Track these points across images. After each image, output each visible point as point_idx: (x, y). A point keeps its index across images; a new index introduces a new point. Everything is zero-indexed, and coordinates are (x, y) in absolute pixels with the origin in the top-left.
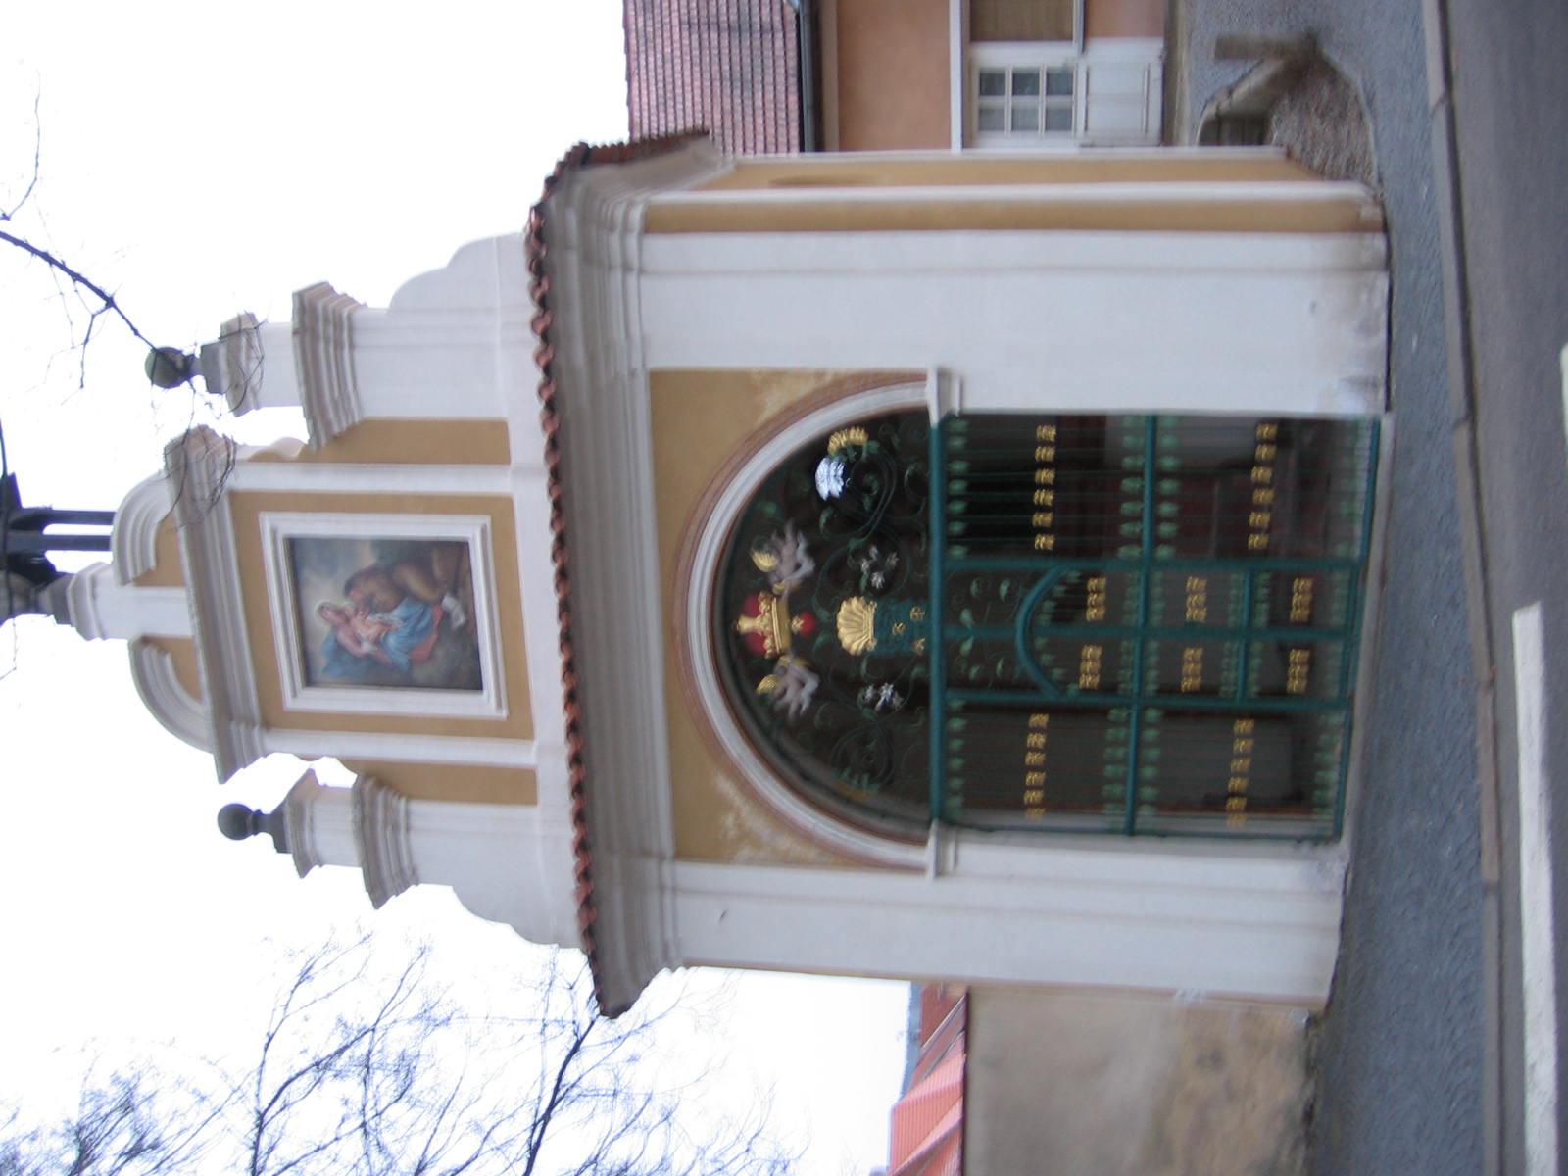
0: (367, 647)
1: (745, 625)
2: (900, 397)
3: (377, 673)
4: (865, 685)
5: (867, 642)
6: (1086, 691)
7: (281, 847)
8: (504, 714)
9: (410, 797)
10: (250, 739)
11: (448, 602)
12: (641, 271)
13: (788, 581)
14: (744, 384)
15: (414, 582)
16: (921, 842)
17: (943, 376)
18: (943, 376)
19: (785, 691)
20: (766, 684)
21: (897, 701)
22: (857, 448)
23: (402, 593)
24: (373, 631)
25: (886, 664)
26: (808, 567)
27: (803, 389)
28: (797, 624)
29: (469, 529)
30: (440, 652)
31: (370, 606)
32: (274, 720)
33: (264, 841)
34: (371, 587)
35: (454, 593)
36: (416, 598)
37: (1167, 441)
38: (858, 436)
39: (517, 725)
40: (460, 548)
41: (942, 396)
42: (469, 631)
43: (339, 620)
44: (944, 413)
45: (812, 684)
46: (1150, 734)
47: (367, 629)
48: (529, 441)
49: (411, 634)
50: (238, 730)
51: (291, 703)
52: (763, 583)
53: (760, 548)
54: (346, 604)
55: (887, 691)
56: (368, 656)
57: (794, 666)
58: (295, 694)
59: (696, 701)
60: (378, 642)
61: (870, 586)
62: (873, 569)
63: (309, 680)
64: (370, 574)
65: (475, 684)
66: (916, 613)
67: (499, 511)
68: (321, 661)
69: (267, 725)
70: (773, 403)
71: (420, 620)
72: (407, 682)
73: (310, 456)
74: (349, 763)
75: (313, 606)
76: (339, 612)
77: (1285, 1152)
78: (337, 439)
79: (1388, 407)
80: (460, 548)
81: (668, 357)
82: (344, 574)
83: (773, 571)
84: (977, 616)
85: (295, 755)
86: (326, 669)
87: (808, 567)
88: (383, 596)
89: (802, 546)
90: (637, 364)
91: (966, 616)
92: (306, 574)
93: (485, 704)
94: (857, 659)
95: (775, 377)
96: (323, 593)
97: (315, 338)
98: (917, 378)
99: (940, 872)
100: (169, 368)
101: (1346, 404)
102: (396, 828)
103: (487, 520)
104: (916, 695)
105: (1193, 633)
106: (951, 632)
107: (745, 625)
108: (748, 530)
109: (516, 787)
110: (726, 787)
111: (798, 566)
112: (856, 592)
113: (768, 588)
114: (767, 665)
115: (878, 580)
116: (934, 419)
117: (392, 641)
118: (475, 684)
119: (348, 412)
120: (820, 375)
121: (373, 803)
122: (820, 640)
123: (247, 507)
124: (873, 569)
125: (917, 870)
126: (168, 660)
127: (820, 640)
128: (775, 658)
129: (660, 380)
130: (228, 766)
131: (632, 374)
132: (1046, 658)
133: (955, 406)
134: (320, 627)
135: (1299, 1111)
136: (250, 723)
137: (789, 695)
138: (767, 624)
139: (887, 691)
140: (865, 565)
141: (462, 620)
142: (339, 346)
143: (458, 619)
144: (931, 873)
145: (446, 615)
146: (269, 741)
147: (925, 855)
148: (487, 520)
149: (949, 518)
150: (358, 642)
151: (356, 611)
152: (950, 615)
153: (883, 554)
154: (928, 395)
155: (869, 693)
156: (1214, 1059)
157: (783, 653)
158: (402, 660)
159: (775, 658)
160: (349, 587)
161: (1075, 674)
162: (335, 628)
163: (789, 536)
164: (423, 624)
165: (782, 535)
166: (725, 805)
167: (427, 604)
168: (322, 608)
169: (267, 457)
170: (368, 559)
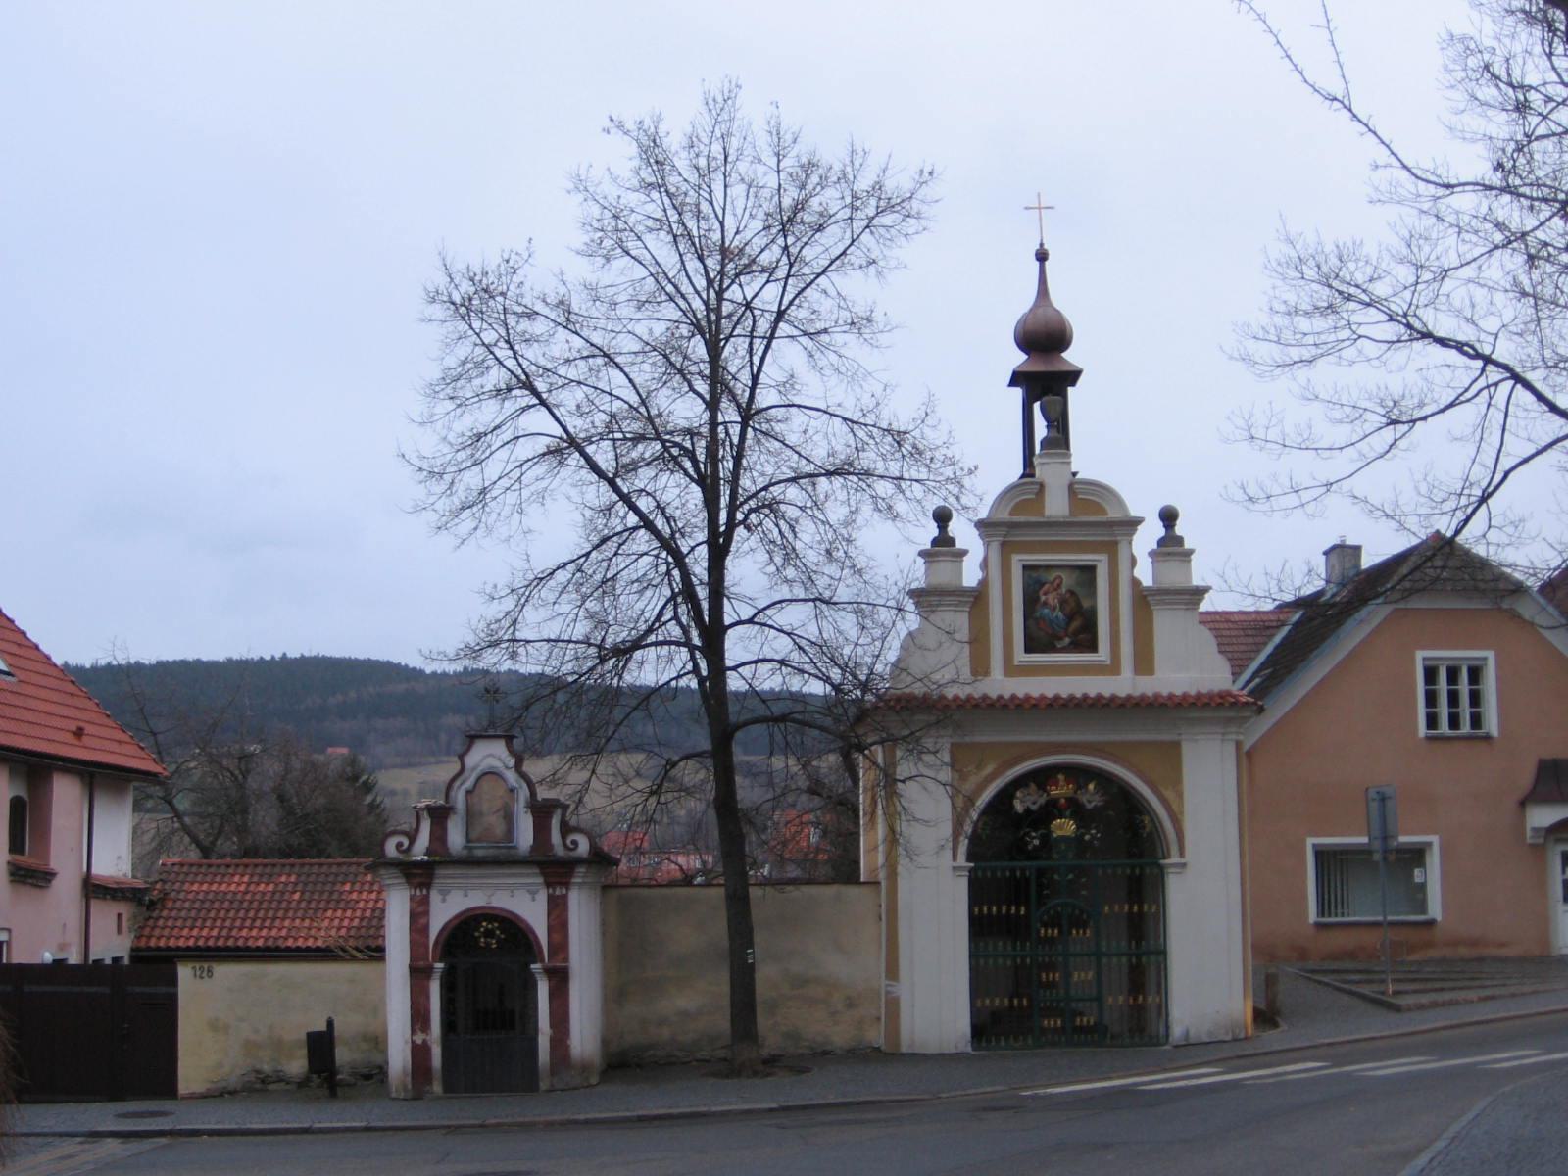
0: (1043, 598)
1: (1061, 777)
2: (1174, 849)
3: (1031, 601)
6: (1038, 932)
9: (970, 612)
10: (999, 535)
11: (1067, 640)
12: (1223, 740)
13: (1084, 798)
14: (1176, 781)
15: (1076, 624)
16: (969, 860)
17: (1184, 866)
18: (1184, 866)
21: (1030, 847)
22: (1144, 827)
23: (1070, 618)
24: (1050, 601)
25: (1046, 839)
26: (1089, 806)
27: (1175, 806)
28: (1063, 801)
29: (1103, 653)
31: (1063, 602)
32: (1007, 549)
34: (1073, 604)
35: (1071, 643)
36: (1068, 624)
37: (1153, 958)
39: (1011, 669)
40: (1092, 647)
42: (1053, 649)
43: (1056, 585)
45: (1034, 807)
46: (1000, 961)
47: (1052, 599)
48: (1146, 686)
50: (1003, 531)
52: (1081, 787)
54: (1064, 590)
55: (1036, 842)
56: (1038, 598)
57: (1042, 800)
59: (1031, 757)
60: (1045, 603)
61: (1083, 835)
63: (1026, 568)
64: (1079, 604)
65: (1028, 650)
67: (1113, 669)
68: (1034, 575)
69: (1003, 544)
70: (1169, 794)
72: (1028, 616)
73: (1135, 583)
74: (984, 583)
75: (1064, 575)
76: (1059, 586)
77: (806, 1043)
78: (1145, 597)
79: (1176, 1046)
80: (1092, 647)
81: (1187, 750)
82: (1078, 590)
87: (1089, 806)
90: (1183, 737)
91: (1071, 876)
92: (1077, 573)
93: (1020, 656)
95: (1180, 795)
96: (1068, 581)
97: (1191, 595)
98: (1182, 854)
99: (954, 869)
100: (1169, 517)
101: (1177, 1031)
102: (956, 605)
103: (1109, 663)
104: (1032, 856)
105: (1068, 975)
107: (1061, 777)
108: (1104, 779)
109: (980, 668)
110: (989, 769)
112: (1078, 828)
113: (1079, 787)
114: (1042, 787)
115: (1087, 837)
116: (1162, 862)
117: (1046, 611)
118: (1028, 650)
119: (1158, 604)
120: (1182, 813)
121: (969, 596)
122: (1056, 811)
123: (1111, 548)
125: (954, 858)
128: (1045, 790)
129: (1176, 746)
130: (983, 526)
131: (1180, 734)
132: (1052, 912)
134: (1052, 576)
135: (829, 1048)
136: (1005, 536)
138: (1061, 790)
140: (1093, 832)
142: (1186, 604)
144: (955, 865)
145: (1061, 639)
146: (995, 546)
147: (962, 860)
148: (1109, 663)
150: (1045, 594)
154: (1175, 859)
155: (1034, 834)
156: (851, 1004)
157: (1048, 794)
158: (1037, 614)
159: (1045, 790)
161: (1045, 926)
162: (1052, 583)
165: (1102, 795)
166: (979, 767)
167: (1066, 629)
168: (1060, 577)
170: (1086, 604)
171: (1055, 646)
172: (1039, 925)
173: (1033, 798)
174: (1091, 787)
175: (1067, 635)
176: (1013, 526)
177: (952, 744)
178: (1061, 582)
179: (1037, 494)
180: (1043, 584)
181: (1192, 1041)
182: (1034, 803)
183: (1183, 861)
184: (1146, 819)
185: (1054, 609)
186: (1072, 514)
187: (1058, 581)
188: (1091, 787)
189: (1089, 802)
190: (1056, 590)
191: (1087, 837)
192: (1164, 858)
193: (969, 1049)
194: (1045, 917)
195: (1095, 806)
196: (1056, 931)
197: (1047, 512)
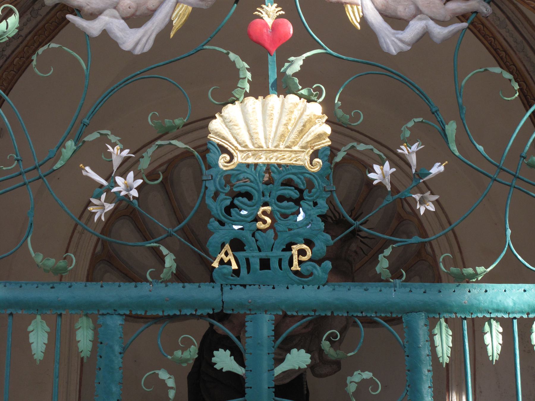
5: (224, 150)
195: (426, 35)
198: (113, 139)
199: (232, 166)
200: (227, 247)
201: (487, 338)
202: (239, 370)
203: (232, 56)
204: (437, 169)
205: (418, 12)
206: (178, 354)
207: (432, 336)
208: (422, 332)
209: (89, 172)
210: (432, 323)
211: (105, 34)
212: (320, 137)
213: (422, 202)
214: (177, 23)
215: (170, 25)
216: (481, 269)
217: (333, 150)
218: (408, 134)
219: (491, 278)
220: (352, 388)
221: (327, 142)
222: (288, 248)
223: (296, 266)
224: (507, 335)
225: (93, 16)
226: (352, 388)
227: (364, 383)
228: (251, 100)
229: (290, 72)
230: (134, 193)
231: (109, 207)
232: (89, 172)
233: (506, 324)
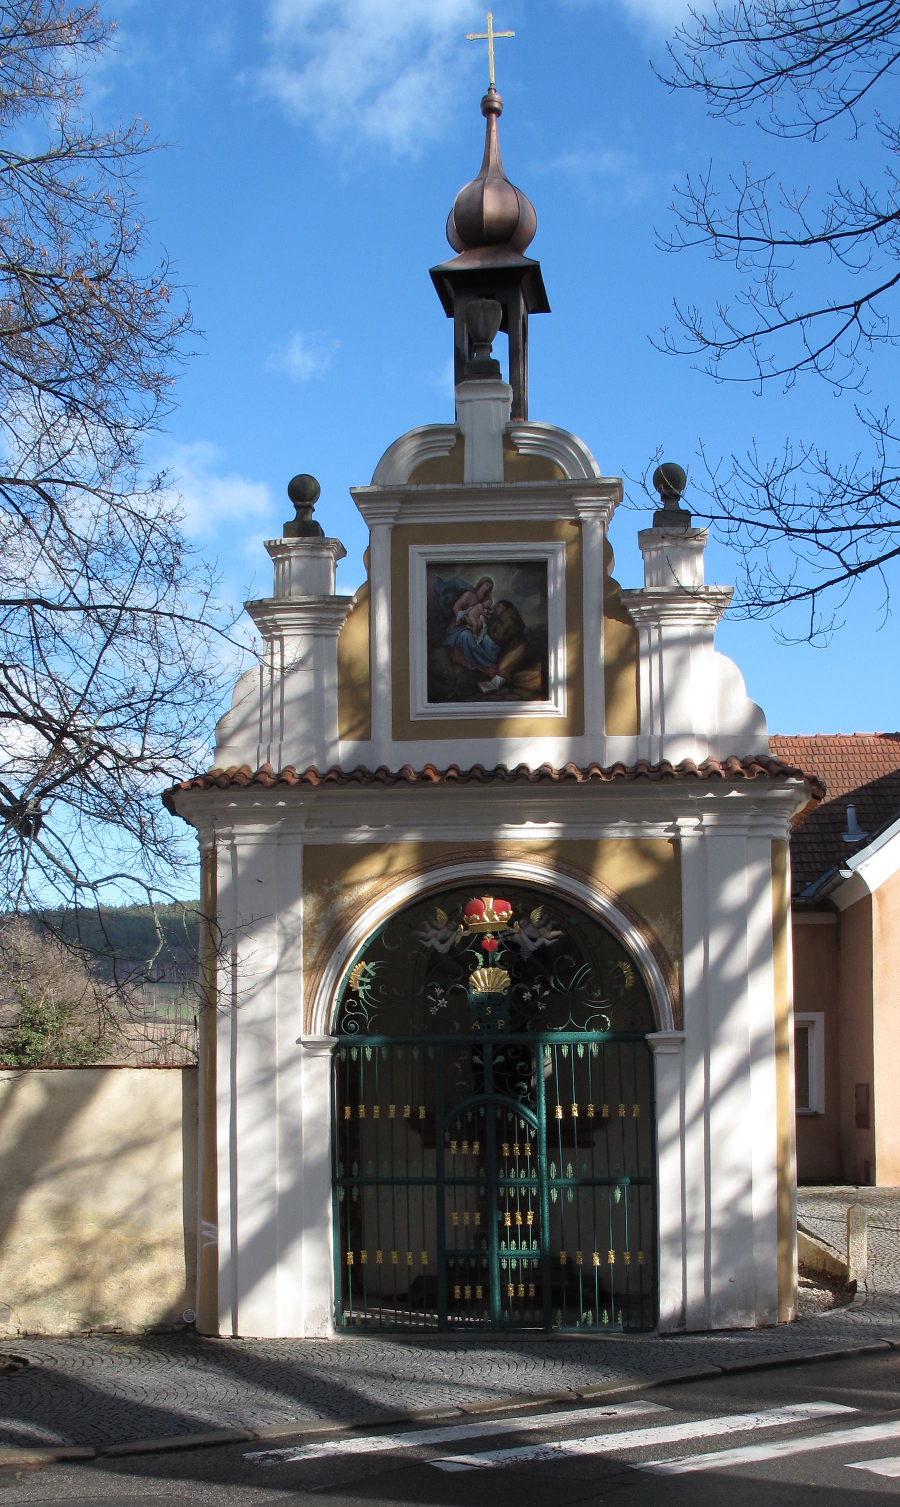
0: (460, 614)
4: (444, 987)
7: (289, 529)
8: (412, 718)
11: (498, 679)
17: (683, 1040)
19: (438, 930)
20: (441, 914)
21: (434, 1010)
24: (472, 618)
26: (532, 946)
30: (458, 671)
31: (492, 620)
33: (290, 513)
34: (508, 622)
35: (503, 685)
36: (500, 656)
38: (629, 981)
41: (668, 1041)
43: (481, 593)
44: (653, 1043)
45: (443, 948)
47: (475, 615)
49: (470, 648)
50: (394, 506)
51: (414, 550)
53: (543, 912)
54: (494, 601)
55: (443, 1003)
56: (453, 615)
58: (421, 554)
60: (464, 622)
61: (521, 992)
62: (534, 993)
65: (433, 697)
66: (501, 1023)
68: (447, 578)
69: (396, 530)
71: (482, 656)
73: (610, 584)
76: (487, 594)
83: (529, 921)
84: (498, 1067)
85: (369, 547)
86: (439, 580)
88: (501, 630)
89: (548, 942)
91: (500, 1059)
92: (517, 572)
94: (466, 981)
98: (680, 1026)
106: (488, 1050)
111: (534, 940)
112: (514, 981)
115: (527, 996)
116: (649, 1036)
117: (465, 634)
118: (433, 697)
124: (534, 993)
125: (308, 1029)
126: (446, 454)
127: (479, 956)
133: (658, 1050)
136: (397, 516)
137: (433, 932)
139: (443, 1003)
140: (537, 987)
141: (484, 690)
143: (485, 686)
145: (489, 678)
146: (384, 534)
149: (573, 1047)
150: (464, 608)
151: (488, 608)
152: (500, 1049)
153: (544, 1000)
154: (668, 1031)
155: (439, 991)
158: (451, 641)
160: (507, 605)
162: (475, 591)
163: (555, 933)
164: (479, 659)
167: (497, 662)
169: (608, 552)
170: (529, 622)
171: (480, 691)
172: (447, 1135)
173: (440, 935)
174: (536, 915)
175: (497, 673)
176: (406, 498)
177: (307, 848)
178: (491, 588)
179: (452, 450)
180: (463, 591)
181: (689, 1327)
182: (443, 942)
183: (679, 1035)
184: (626, 967)
185: (479, 630)
186: (506, 480)
187: (485, 587)
188: (536, 915)
189: (534, 940)
190: (481, 601)
191: (527, 996)
192: (654, 1030)
193: (329, 1332)
194: (459, 1124)
196: (476, 1146)
197: (467, 478)
198: (437, 984)
199: (477, 993)
200: (477, 1022)
201: (563, 1050)
202: (481, 1063)
203: (477, 954)
204: (547, 993)
205: (541, 936)
206: (461, 1058)
207: (544, 1050)
208: (541, 1049)
209: (429, 997)
210: (545, 1046)
211: (432, 946)
212: (506, 982)
213: (541, 1005)
214: (457, 942)
215: (455, 942)
216: (560, 1028)
217: (511, 987)
218: (536, 981)
219: (563, 1030)
220: (518, 1068)
221: (509, 984)
222: (496, 1022)
223: (499, 1028)
224: (569, 1049)
225: (427, 940)
226: (518, 1068)
227: (522, 1067)
228: (483, 969)
229: (496, 960)
230: (445, 1006)
231: (437, 1010)
232: (429, 997)
233: (569, 1045)
